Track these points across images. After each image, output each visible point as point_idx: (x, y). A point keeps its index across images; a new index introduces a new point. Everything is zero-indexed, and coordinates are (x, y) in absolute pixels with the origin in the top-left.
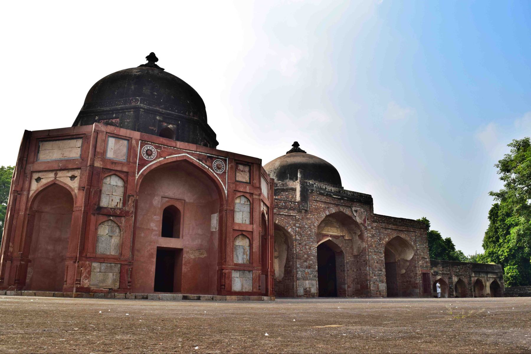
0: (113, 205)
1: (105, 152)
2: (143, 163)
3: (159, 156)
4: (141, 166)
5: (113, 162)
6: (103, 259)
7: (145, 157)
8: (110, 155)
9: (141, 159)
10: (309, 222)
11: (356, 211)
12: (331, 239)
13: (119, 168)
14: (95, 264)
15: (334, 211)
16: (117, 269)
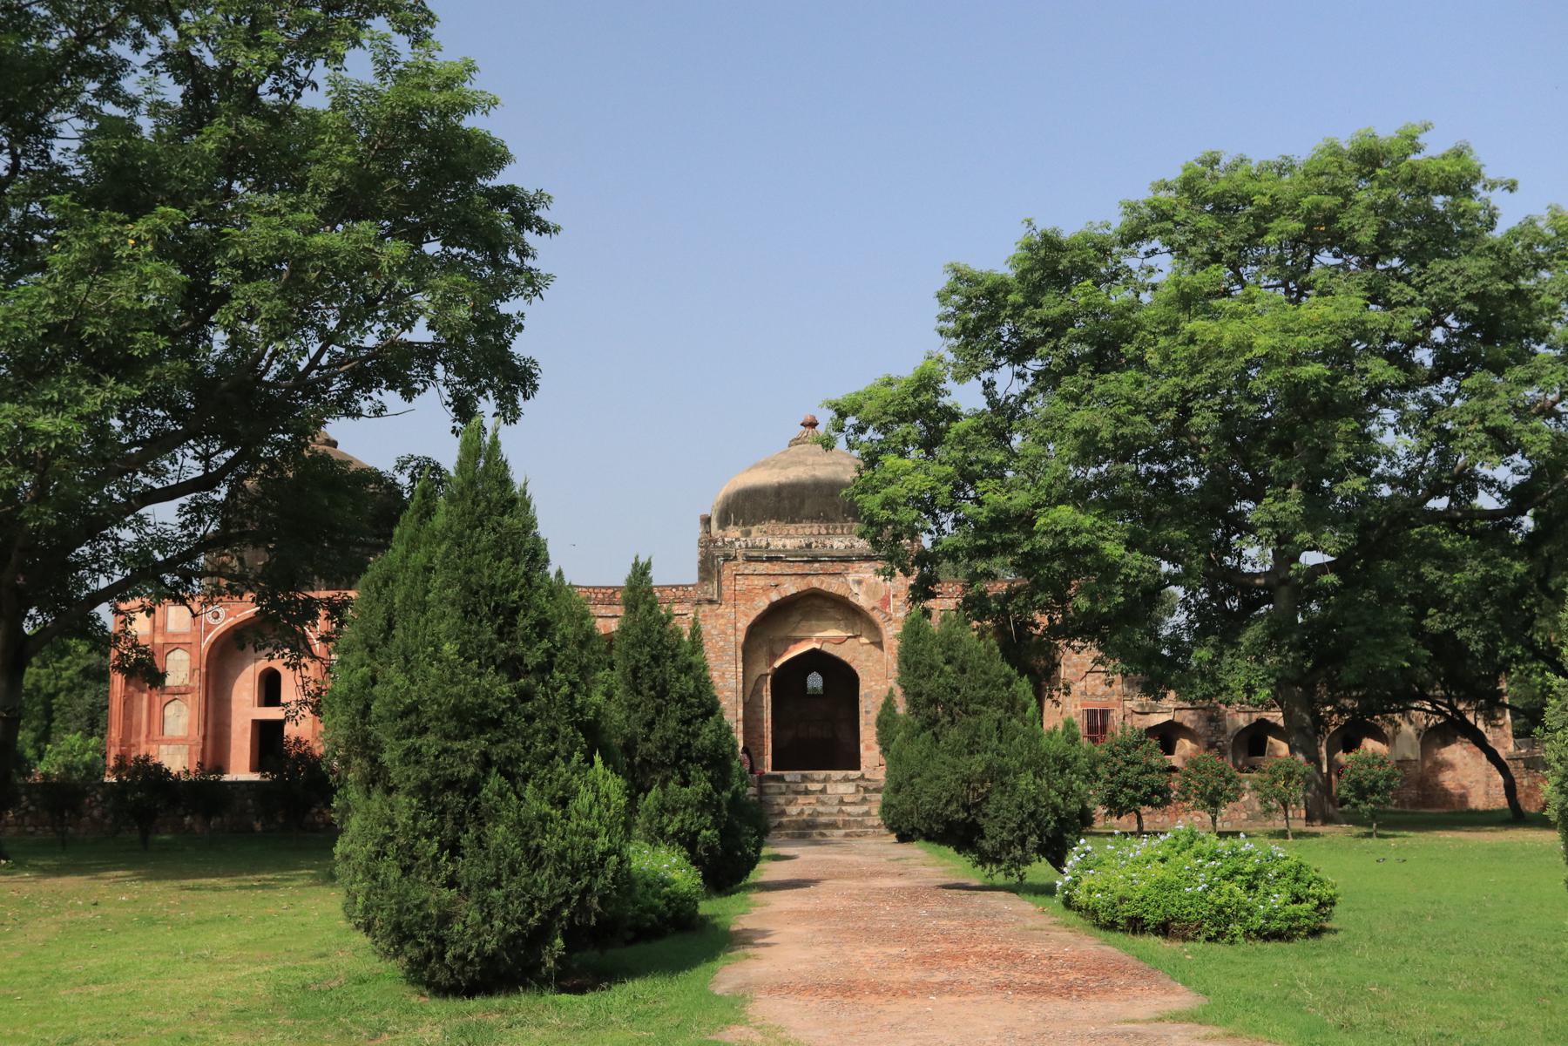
0: (178, 682)
1: (165, 625)
2: (209, 628)
3: (228, 615)
4: (208, 632)
5: (175, 635)
6: (171, 741)
7: (212, 621)
8: (171, 627)
9: (207, 624)
10: (722, 621)
11: (859, 582)
12: (818, 646)
13: (181, 640)
14: (163, 747)
15: (793, 590)
16: (185, 749)
